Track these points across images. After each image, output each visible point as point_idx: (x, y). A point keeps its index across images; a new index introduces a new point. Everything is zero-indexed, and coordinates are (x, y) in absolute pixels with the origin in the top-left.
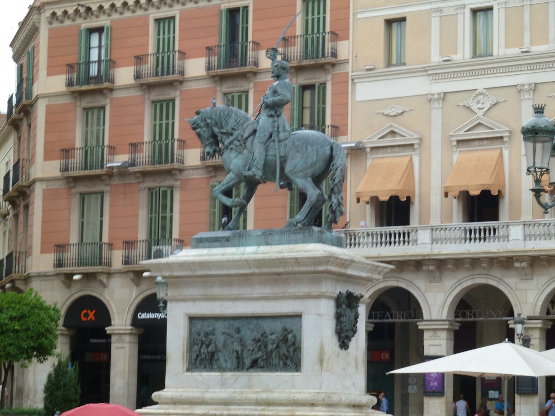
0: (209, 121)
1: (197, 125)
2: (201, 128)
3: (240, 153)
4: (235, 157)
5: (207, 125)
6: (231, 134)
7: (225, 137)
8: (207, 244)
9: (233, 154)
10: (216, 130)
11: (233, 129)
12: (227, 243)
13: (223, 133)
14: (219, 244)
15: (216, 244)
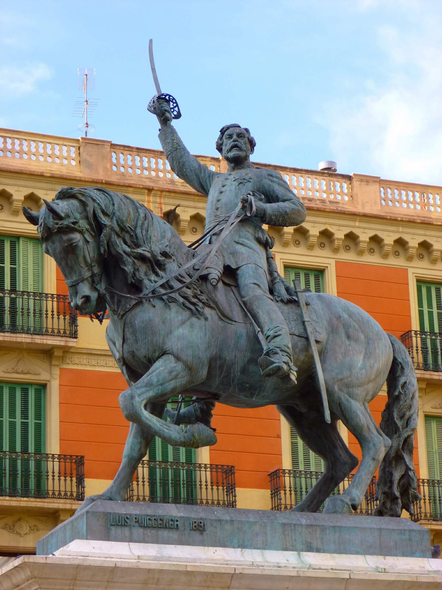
0: (104, 220)
1: (74, 223)
2: (81, 232)
3: (197, 314)
4: (183, 323)
5: (98, 227)
6: (161, 266)
7: (143, 268)
8: (138, 531)
9: (175, 314)
10: (122, 247)
11: (165, 254)
12: (196, 535)
13: (142, 258)
14: (174, 535)
15: (165, 533)
